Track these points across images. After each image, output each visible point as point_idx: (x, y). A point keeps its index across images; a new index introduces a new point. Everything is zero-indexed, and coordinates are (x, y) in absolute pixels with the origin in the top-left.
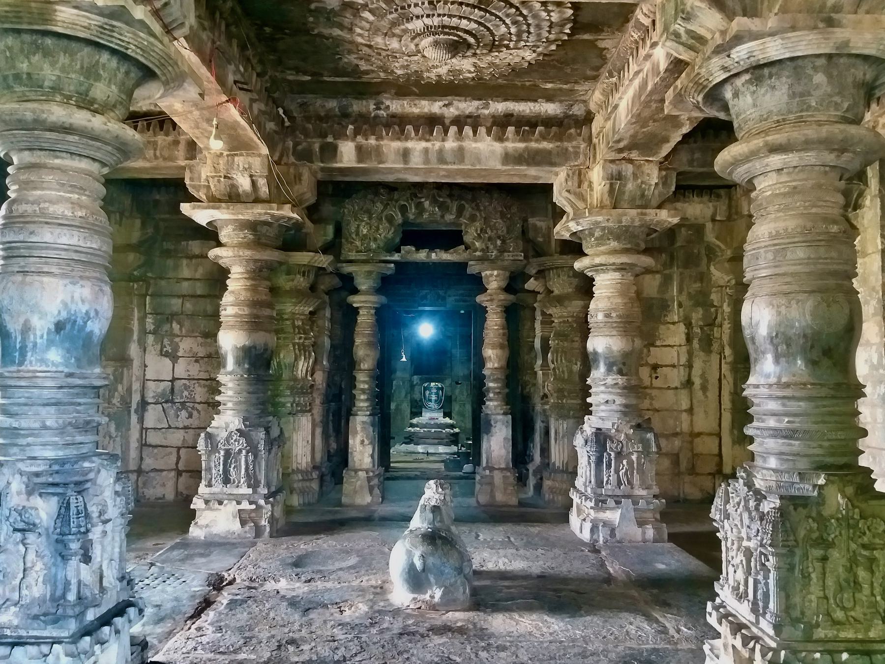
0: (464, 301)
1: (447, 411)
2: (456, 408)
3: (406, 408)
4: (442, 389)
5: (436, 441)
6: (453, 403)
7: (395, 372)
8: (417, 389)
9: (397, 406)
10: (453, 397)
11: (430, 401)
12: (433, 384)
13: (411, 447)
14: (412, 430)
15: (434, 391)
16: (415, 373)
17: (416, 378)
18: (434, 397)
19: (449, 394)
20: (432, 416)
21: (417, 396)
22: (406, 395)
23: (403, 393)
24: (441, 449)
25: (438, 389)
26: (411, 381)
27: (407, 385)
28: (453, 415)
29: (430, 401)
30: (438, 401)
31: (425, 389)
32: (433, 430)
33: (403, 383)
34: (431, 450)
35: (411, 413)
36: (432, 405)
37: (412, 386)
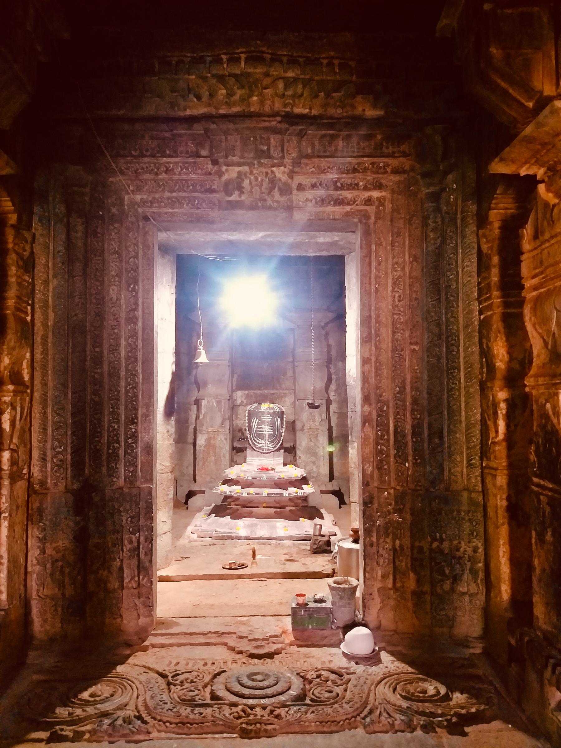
0: (339, 202)
1: (287, 445)
2: (303, 442)
3: (223, 443)
4: (282, 414)
5: (273, 510)
6: (299, 435)
7: (205, 384)
8: (240, 410)
9: (208, 440)
10: (298, 425)
11: (260, 436)
12: (264, 407)
13: (225, 524)
14: (226, 489)
15: (267, 418)
16: (240, 387)
17: (240, 396)
18: (267, 430)
19: (292, 418)
20: (263, 465)
21: (242, 421)
22: (222, 423)
23: (219, 420)
24: (282, 528)
25: (274, 414)
26: (231, 399)
27: (225, 405)
28: (298, 453)
29: (260, 436)
30: (275, 436)
31: (251, 415)
32: (265, 492)
33: (219, 402)
34: (263, 528)
35: (234, 448)
36: (264, 444)
37: (233, 408)
